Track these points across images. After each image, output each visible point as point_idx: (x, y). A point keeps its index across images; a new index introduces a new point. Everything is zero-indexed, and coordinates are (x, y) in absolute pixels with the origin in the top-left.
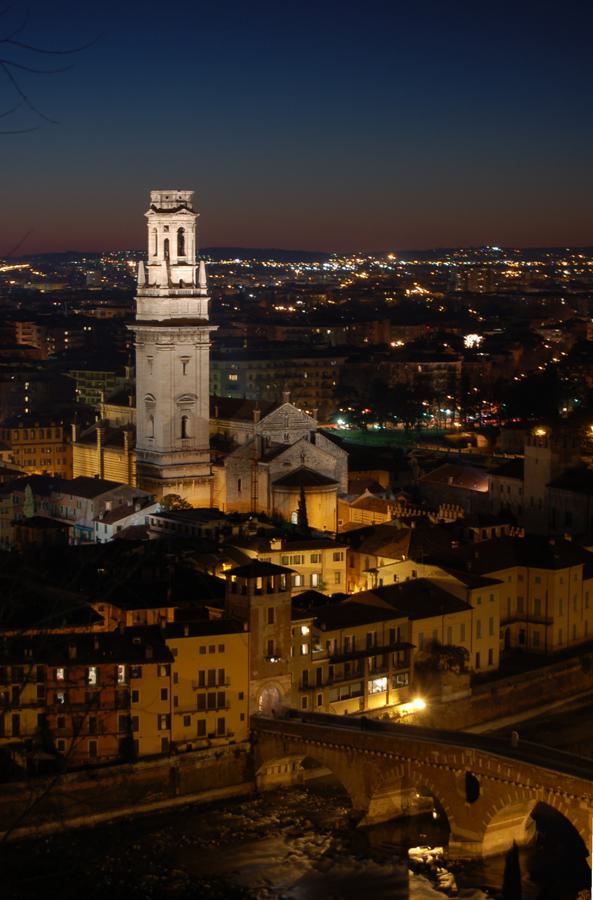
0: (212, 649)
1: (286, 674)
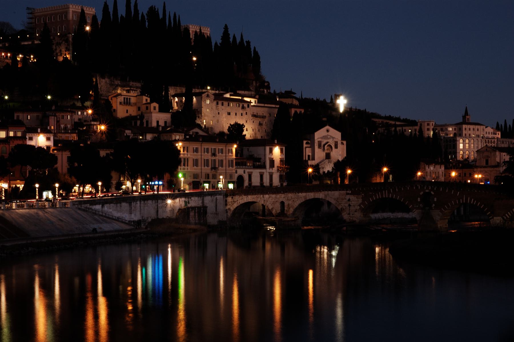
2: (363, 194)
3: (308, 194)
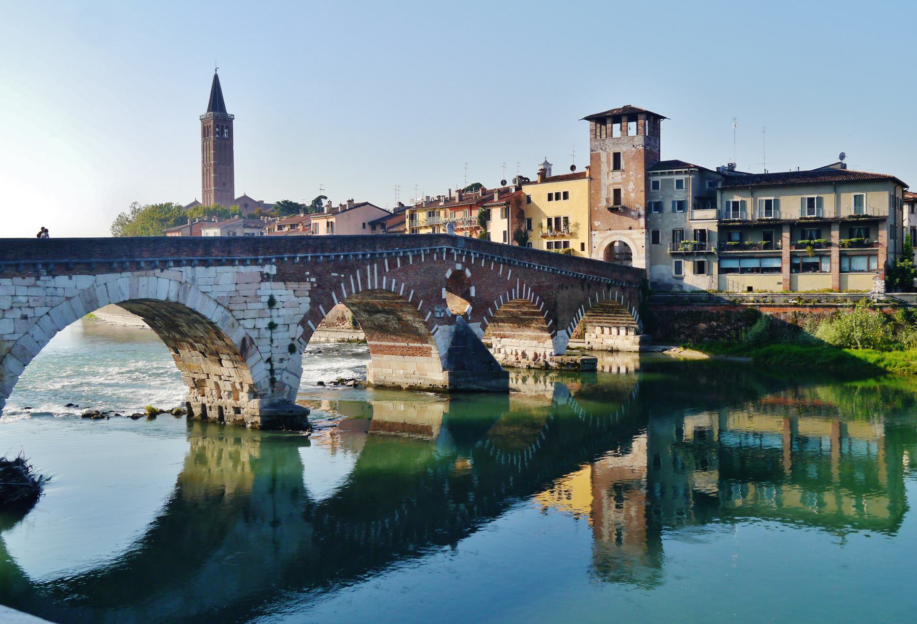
0: (558, 196)
1: (639, 228)
2: (313, 280)
3: (101, 278)
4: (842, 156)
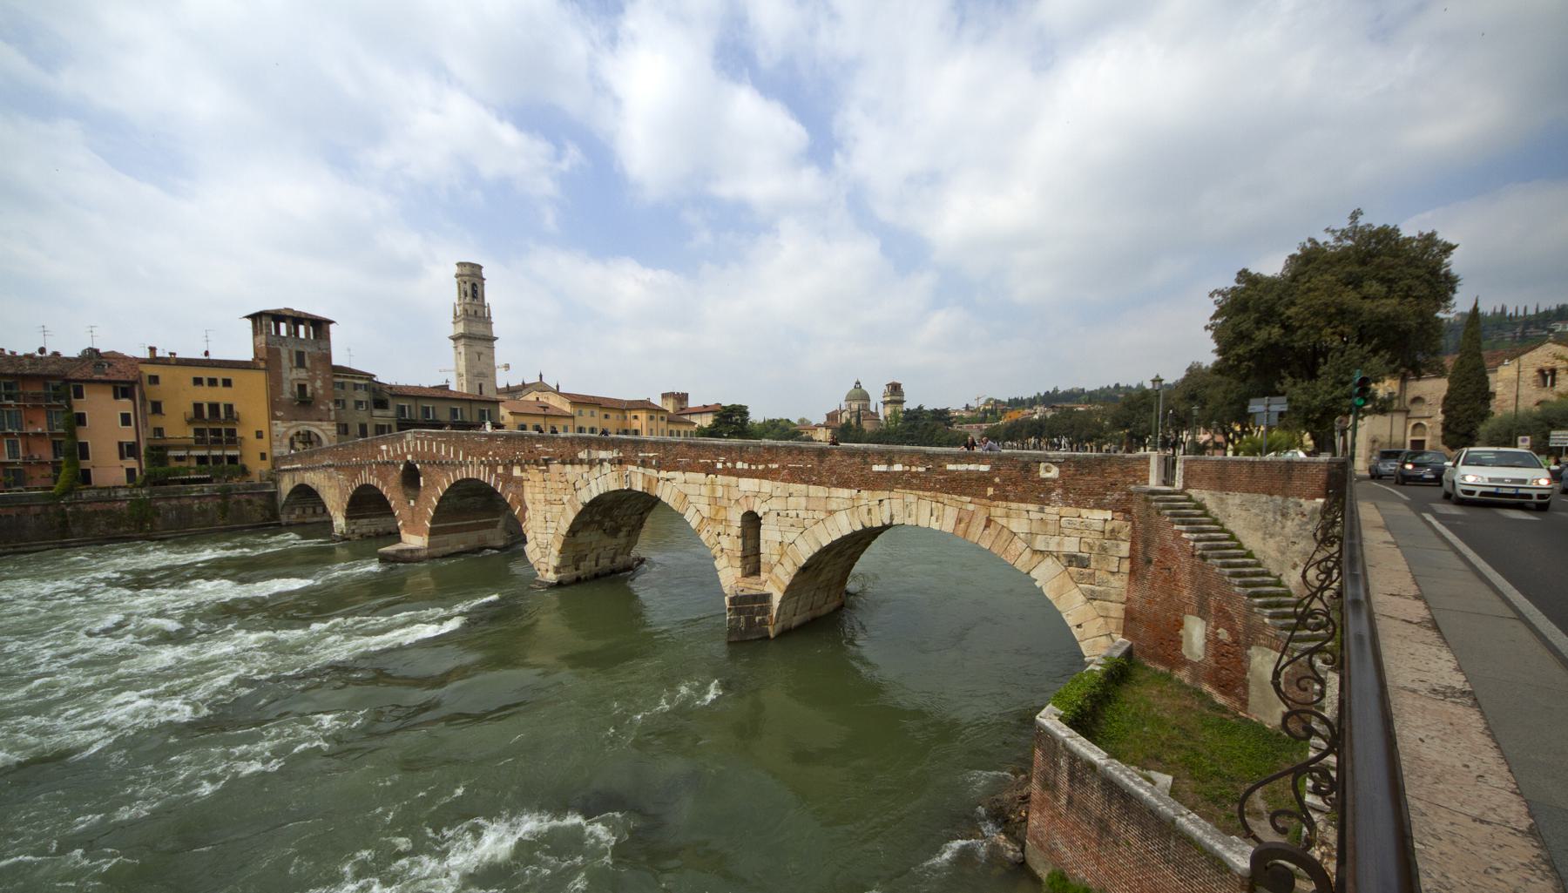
0: (213, 382)
4: (447, 381)
